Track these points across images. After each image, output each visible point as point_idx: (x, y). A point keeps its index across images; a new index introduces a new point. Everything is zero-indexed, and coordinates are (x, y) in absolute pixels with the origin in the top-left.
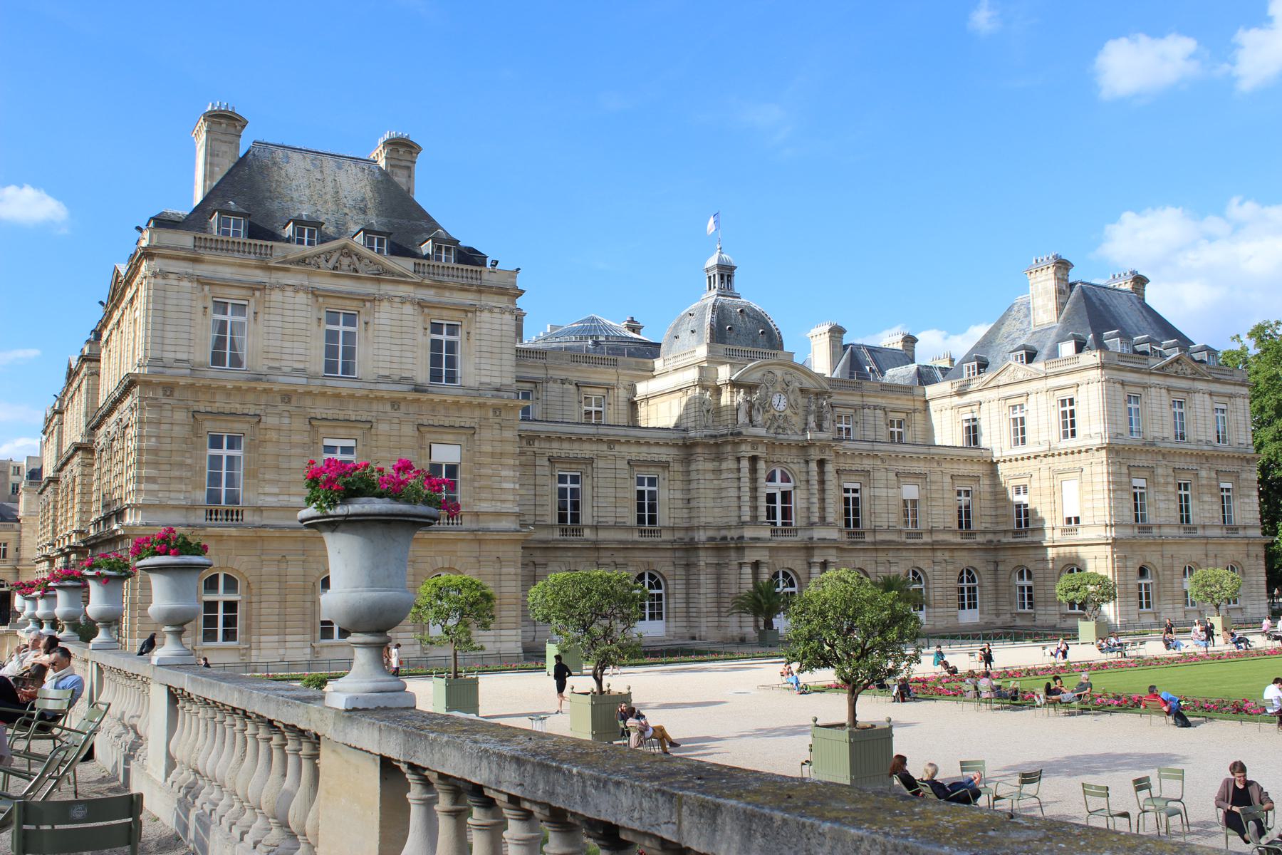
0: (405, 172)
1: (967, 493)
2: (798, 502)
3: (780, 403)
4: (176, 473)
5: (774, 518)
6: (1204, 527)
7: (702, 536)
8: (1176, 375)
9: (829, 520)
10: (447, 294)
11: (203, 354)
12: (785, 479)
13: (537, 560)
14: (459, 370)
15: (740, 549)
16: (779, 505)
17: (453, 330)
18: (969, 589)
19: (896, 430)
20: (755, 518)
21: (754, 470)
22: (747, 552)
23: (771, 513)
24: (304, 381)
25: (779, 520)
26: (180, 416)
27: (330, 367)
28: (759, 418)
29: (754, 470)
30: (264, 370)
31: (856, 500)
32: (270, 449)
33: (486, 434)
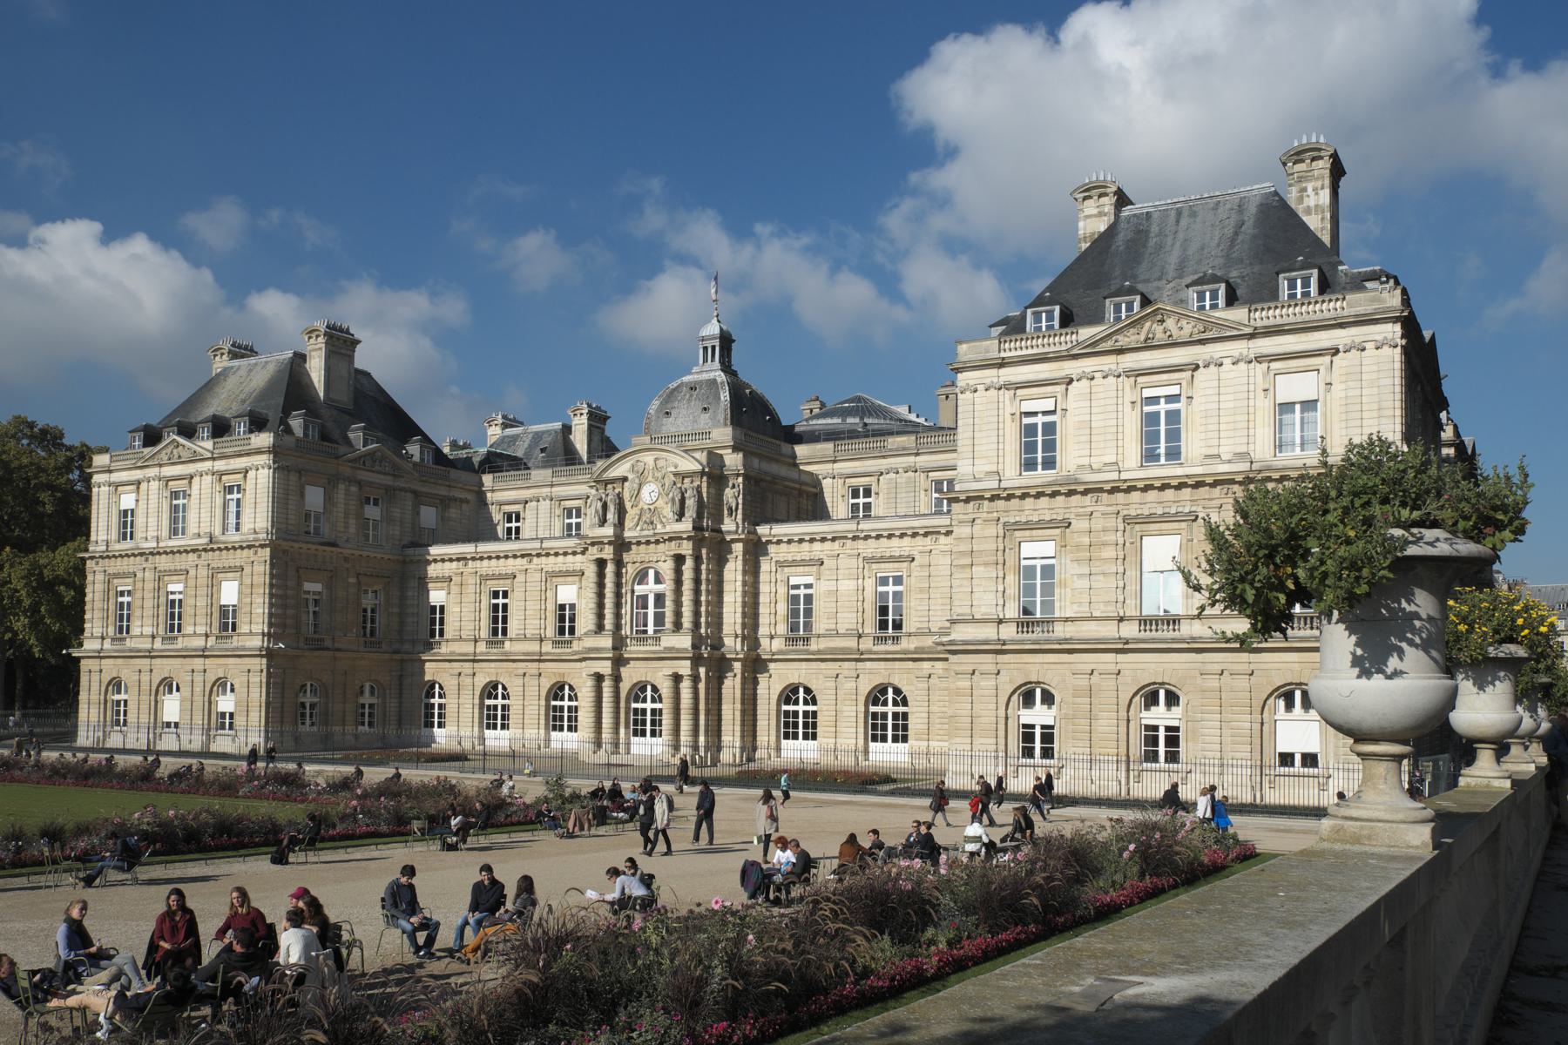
3: (649, 493)
8: (1148, 346)
9: (687, 621)
12: (658, 580)
16: (651, 611)
20: (600, 627)
21: (601, 575)
25: (651, 628)
28: (611, 516)
29: (601, 575)
31: (809, 599)
33: (247, 570)
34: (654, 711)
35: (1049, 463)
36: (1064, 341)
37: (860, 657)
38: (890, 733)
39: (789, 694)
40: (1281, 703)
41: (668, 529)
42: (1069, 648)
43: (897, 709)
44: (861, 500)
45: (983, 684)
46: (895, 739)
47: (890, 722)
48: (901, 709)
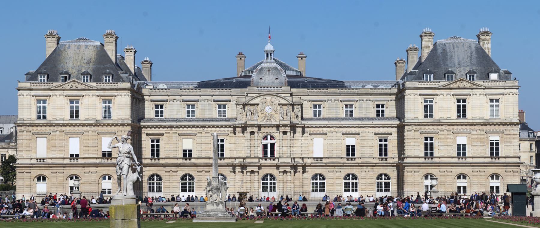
0: (112, 44)
1: (386, 140)
2: (277, 148)
3: (268, 110)
4: (28, 149)
5: (267, 154)
6: (472, 157)
7: (237, 161)
10: (107, 91)
11: (34, 115)
12: (272, 138)
13: (173, 170)
14: (112, 114)
15: (246, 166)
16: (269, 149)
17: (109, 102)
18: (385, 183)
19: (380, 109)
22: (248, 168)
23: (265, 152)
24: (62, 122)
26: (29, 134)
27: (72, 117)
30: (51, 119)
32: (53, 141)
34: (271, 184)
35: (431, 116)
36: (436, 85)
37: (342, 165)
38: (351, 189)
39: (314, 177)
40: (490, 178)
41: (281, 123)
42: (439, 165)
43: (353, 181)
44: (317, 109)
45: (415, 174)
46: (353, 191)
47: (351, 185)
48: (355, 181)
